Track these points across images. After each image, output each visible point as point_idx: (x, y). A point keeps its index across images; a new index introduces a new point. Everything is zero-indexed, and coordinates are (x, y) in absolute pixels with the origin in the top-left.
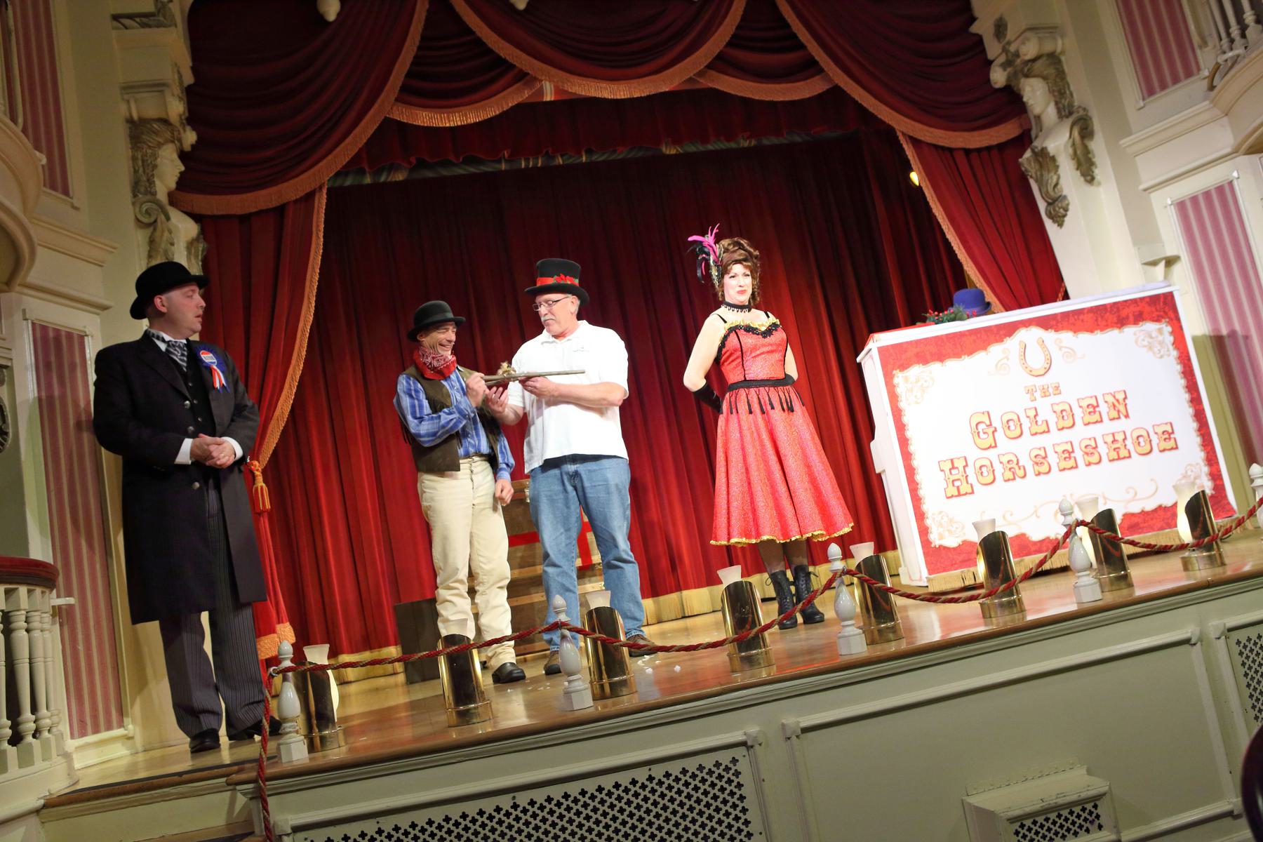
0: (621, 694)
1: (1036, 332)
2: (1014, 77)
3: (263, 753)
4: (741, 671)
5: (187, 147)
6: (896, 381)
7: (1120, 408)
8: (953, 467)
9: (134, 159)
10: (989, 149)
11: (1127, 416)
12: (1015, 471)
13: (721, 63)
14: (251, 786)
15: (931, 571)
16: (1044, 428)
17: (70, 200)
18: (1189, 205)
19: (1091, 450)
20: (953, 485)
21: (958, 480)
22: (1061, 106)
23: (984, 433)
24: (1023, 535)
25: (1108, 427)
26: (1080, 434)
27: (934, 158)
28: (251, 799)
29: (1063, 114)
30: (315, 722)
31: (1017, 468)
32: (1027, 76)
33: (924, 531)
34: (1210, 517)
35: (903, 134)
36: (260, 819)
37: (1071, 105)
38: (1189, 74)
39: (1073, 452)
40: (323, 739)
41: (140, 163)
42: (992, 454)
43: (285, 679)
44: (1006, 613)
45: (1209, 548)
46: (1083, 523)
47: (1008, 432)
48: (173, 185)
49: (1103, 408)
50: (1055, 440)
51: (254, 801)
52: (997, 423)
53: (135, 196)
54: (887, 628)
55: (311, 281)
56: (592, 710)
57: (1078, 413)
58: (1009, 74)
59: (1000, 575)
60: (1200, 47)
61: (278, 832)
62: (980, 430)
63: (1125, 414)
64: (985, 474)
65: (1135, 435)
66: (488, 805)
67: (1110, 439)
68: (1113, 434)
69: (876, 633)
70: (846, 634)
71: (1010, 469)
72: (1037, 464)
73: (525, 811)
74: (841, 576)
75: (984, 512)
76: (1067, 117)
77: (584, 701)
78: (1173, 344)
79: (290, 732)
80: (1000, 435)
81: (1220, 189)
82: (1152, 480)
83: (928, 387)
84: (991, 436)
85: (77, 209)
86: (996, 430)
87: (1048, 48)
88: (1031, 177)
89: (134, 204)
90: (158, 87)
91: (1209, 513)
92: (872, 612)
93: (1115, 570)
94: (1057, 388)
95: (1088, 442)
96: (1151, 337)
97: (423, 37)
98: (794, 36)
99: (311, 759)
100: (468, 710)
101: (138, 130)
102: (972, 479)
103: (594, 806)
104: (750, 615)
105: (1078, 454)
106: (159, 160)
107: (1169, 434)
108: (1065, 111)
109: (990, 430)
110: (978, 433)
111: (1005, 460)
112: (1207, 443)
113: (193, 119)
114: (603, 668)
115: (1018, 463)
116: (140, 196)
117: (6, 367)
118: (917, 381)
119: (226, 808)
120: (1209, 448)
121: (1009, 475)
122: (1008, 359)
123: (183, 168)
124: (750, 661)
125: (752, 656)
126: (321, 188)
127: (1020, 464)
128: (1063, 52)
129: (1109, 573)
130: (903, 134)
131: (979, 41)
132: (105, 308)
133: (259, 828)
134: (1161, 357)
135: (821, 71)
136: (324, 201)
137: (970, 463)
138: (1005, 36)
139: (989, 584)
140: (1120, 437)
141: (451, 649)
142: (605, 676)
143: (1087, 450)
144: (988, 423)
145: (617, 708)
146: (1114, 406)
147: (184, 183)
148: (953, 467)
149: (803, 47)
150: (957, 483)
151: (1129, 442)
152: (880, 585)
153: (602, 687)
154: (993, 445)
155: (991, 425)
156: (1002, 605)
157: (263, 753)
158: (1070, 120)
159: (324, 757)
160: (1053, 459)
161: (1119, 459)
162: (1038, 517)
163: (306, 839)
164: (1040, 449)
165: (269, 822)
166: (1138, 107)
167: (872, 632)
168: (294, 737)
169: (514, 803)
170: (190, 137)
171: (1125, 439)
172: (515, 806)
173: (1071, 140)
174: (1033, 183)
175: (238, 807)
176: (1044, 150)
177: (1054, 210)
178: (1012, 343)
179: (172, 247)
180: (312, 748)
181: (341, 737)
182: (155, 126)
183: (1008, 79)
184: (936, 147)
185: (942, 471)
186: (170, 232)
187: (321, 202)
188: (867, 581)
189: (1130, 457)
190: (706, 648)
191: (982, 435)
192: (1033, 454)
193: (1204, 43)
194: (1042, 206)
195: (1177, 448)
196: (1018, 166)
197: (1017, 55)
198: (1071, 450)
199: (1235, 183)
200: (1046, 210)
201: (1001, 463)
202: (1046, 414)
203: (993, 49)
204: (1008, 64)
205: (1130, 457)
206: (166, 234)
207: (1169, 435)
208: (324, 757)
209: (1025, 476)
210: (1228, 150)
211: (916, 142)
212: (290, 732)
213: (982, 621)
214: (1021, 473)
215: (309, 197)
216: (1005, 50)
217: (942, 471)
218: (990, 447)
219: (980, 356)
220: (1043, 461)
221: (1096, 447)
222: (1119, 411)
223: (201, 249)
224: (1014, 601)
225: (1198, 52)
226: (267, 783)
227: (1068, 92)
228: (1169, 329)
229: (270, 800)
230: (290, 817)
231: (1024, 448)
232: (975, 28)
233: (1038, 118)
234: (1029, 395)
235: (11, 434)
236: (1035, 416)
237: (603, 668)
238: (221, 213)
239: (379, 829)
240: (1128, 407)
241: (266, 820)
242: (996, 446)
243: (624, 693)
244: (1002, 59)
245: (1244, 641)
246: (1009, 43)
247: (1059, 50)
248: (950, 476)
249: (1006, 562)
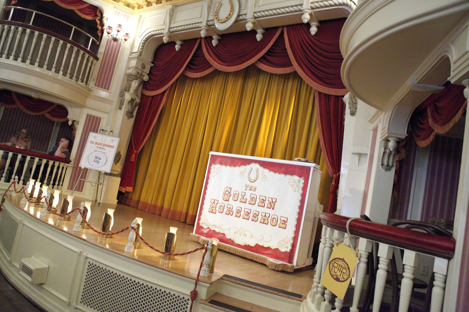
1: (257, 166)
6: (212, 167)
7: (272, 205)
11: (273, 209)
12: (230, 212)
16: (245, 201)
19: (256, 216)
21: (213, 207)
23: (227, 195)
24: (43, 192)
25: (265, 210)
26: (255, 208)
31: (231, 211)
39: (250, 214)
42: (226, 203)
49: (267, 202)
50: (255, 208)
52: (232, 193)
57: (258, 200)
62: (226, 193)
63: (273, 208)
64: (274, 221)
65: (273, 217)
67: (264, 214)
68: (266, 213)
71: (229, 210)
72: (254, 216)
78: (302, 188)
80: (231, 198)
82: (271, 236)
83: (218, 173)
84: (229, 196)
86: (230, 196)
94: (255, 189)
95: (256, 213)
96: (295, 182)
102: (217, 209)
105: (251, 215)
107: (285, 222)
109: (229, 195)
111: (229, 206)
112: (297, 232)
115: (232, 210)
120: (296, 234)
121: (228, 212)
127: (233, 210)
134: (295, 191)
135: (292, 65)
140: (267, 215)
143: (238, 211)
144: (230, 192)
146: (271, 203)
148: (214, 203)
150: (213, 208)
151: (270, 219)
160: (242, 213)
161: (263, 223)
162: (229, 231)
164: (240, 208)
171: (269, 217)
178: (248, 167)
185: (211, 202)
189: (267, 224)
191: (226, 195)
195: (285, 229)
198: (249, 213)
201: (244, 211)
202: (248, 197)
205: (267, 224)
207: (285, 222)
209: (232, 215)
217: (211, 202)
219: (237, 168)
220: (240, 213)
221: (258, 215)
222: (271, 206)
228: (303, 181)
231: (236, 205)
234: (245, 187)
236: (244, 196)
240: (275, 205)
242: (228, 201)
245: (91, 263)
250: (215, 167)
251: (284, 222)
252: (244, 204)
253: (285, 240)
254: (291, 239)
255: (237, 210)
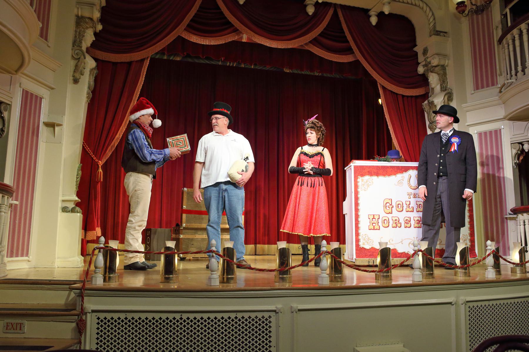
0: (230, 282)
2: (427, 71)
3: (86, 279)
4: (279, 282)
5: (98, 31)
6: (358, 180)
8: (374, 218)
9: (76, 31)
10: (412, 97)
12: (397, 224)
13: (315, 42)
14: (79, 291)
15: (357, 256)
16: (412, 209)
17: (47, 42)
18: (483, 135)
20: (372, 225)
21: (375, 223)
22: (442, 86)
23: (389, 207)
27: (391, 96)
28: (77, 296)
29: (443, 89)
30: (108, 270)
31: (398, 223)
32: (432, 72)
33: (357, 241)
34: (468, 257)
35: (380, 84)
36: (79, 305)
37: (446, 87)
38: (493, 85)
40: (109, 278)
41: (78, 34)
42: (390, 216)
43: (99, 252)
44: (385, 279)
45: (466, 269)
46: (421, 251)
47: (397, 209)
48: (89, 45)
51: (78, 297)
52: (394, 204)
53: (73, 46)
54: (338, 277)
55: (136, 94)
56: (218, 287)
58: (425, 70)
59: (385, 264)
60: (499, 75)
61: (86, 311)
64: (386, 223)
66: (171, 316)
69: (333, 278)
70: (322, 276)
71: (395, 223)
73: (185, 321)
74: (325, 253)
75: (382, 238)
76: (444, 91)
77: (216, 283)
79: (98, 273)
80: (394, 209)
81: (496, 131)
83: (370, 185)
84: (391, 208)
85: (49, 47)
86: (393, 207)
87: (442, 63)
88: (426, 111)
89: (72, 49)
90: (92, 5)
91: (468, 255)
92: (333, 269)
93: (429, 271)
97: (200, 7)
98: (345, 37)
99: (104, 285)
100: (169, 277)
101: (80, 20)
102: (380, 224)
103: (212, 324)
104: (287, 262)
106: (86, 34)
108: (444, 89)
109: (391, 207)
110: (386, 206)
113: (102, 20)
114: (225, 271)
115: (399, 221)
116: (75, 47)
117: (9, 105)
118: (367, 182)
119: (66, 297)
122: (403, 180)
123: (94, 39)
124: (283, 279)
125: (284, 277)
126: (147, 58)
128: (447, 66)
129: (426, 272)
130: (380, 84)
131: (416, 54)
132: (52, 89)
133: (79, 308)
136: (148, 64)
137: (381, 218)
138: (427, 55)
139: (380, 267)
141: (168, 252)
142: (225, 274)
144: (391, 204)
145: (229, 288)
147: (93, 45)
148: (374, 218)
149: (347, 42)
150: (374, 225)
152: (339, 260)
153: (223, 278)
154: (391, 212)
155: (391, 204)
156: (383, 276)
157: (86, 279)
158: (445, 93)
159: (109, 285)
162: (402, 244)
163: (96, 316)
165: (83, 306)
166: (471, 93)
167: (332, 277)
168: (99, 275)
169: (181, 317)
170: (100, 27)
172: (181, 319)
173: (444, 100)
174: (425, 113)
175: (70, 298)
176: (433, 102)
177: (432, 126)
179: (84, 70)
180: (105, 280)
181: (117, 278)
182: (87, 20)
183: (424, 71)
184: (392, 92)
186: (85, 63)
187: (147, 63)
188: (334, 257)
190: (267, 271)
191: (387, 208)
192: (405, 219)
193: (501, 75)
194: (427, 123)
196: (422, 105)
197: (430, 63)
199: (502, 130)
200: (429, 125)
203: (421, 58)
204: (425, 66)
206: (83, 64)
208: (109, 285)
209: (400, 227)
210: (502, 117)
211: (384, 88)
212: (98, 273)
213: (375, 280)
214: (399, 225)
215: (142, 61)
216: (425, 60)
217: (369, 218)
218: (390, 213)
219: (393, 177)
220: (409, 222)
223: (95, 72)
224: (389, 275)
225: (498, 77)
226: (85, 291)
227: (446, 81)
229: (85, 298)
230: (91, 306)
232: (415, 49)
233: (433, 89)
234: (408, 196)
235: (5, 132)
237: (225, 271)
238: (106, 60)
239: (126, 317)
241: (82, 305)
242: (392, 213)
243: (232, 282)
244: (424, 63)
246: (427, 58)
247: (446, 64)
248: (372, 221)
249: (388, 259)
250: (363, 179)
251: (418, 222)
252: (411, 213)
253: (370, 241)
254: (468, 235)
255: (405, 221)
